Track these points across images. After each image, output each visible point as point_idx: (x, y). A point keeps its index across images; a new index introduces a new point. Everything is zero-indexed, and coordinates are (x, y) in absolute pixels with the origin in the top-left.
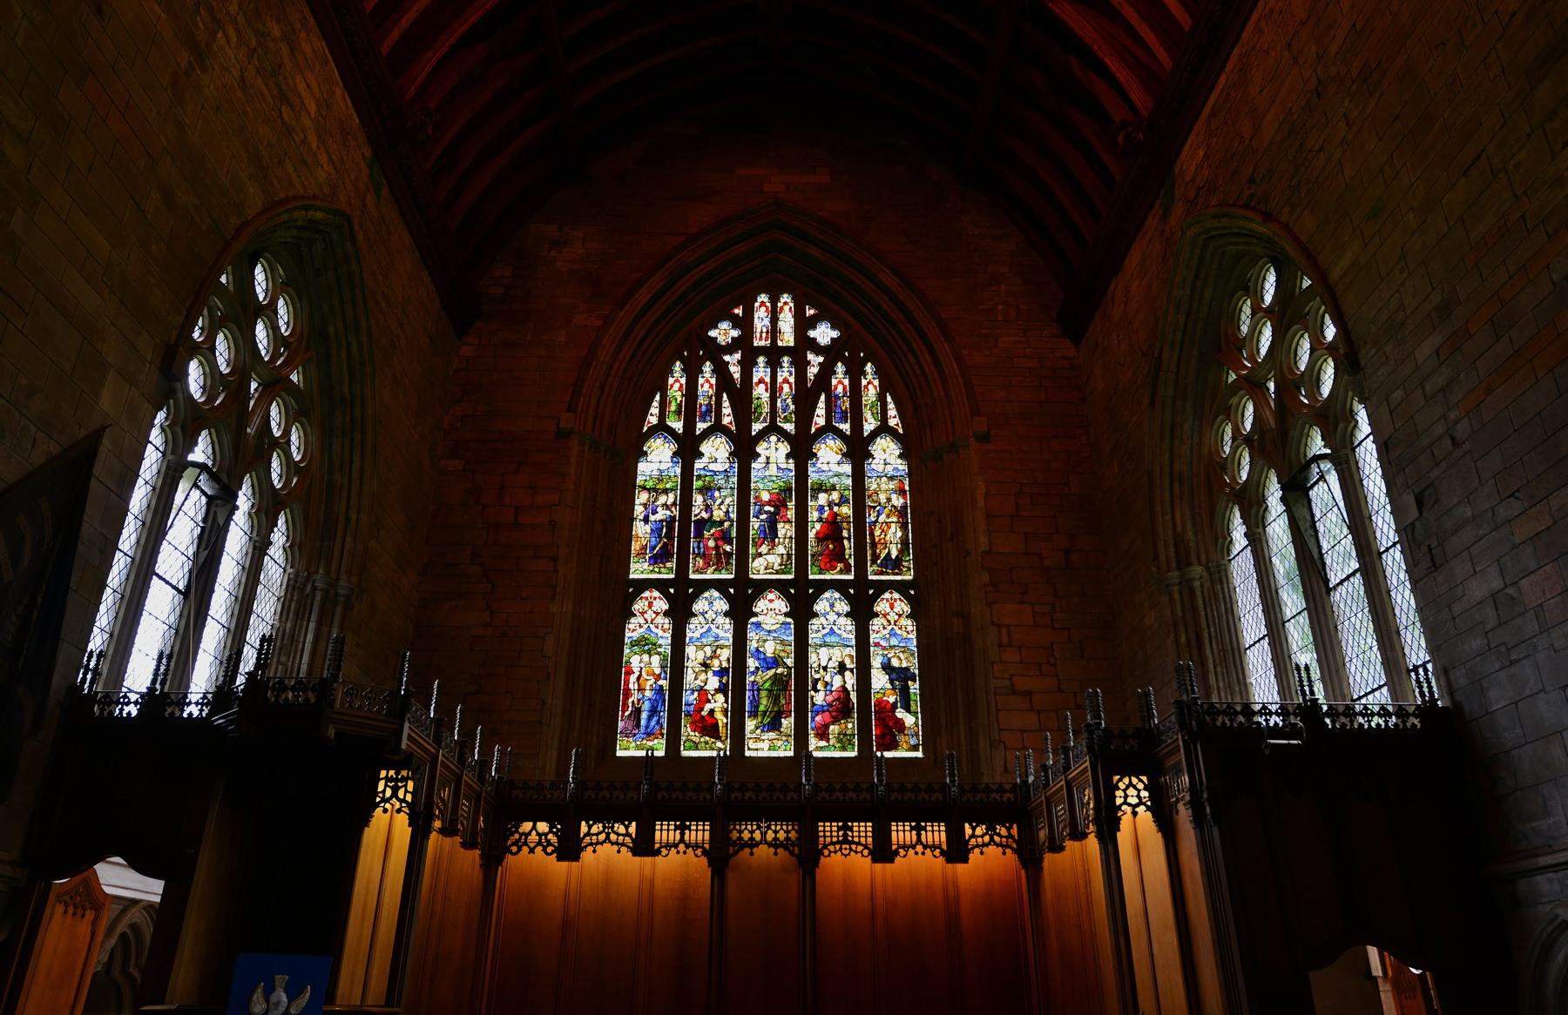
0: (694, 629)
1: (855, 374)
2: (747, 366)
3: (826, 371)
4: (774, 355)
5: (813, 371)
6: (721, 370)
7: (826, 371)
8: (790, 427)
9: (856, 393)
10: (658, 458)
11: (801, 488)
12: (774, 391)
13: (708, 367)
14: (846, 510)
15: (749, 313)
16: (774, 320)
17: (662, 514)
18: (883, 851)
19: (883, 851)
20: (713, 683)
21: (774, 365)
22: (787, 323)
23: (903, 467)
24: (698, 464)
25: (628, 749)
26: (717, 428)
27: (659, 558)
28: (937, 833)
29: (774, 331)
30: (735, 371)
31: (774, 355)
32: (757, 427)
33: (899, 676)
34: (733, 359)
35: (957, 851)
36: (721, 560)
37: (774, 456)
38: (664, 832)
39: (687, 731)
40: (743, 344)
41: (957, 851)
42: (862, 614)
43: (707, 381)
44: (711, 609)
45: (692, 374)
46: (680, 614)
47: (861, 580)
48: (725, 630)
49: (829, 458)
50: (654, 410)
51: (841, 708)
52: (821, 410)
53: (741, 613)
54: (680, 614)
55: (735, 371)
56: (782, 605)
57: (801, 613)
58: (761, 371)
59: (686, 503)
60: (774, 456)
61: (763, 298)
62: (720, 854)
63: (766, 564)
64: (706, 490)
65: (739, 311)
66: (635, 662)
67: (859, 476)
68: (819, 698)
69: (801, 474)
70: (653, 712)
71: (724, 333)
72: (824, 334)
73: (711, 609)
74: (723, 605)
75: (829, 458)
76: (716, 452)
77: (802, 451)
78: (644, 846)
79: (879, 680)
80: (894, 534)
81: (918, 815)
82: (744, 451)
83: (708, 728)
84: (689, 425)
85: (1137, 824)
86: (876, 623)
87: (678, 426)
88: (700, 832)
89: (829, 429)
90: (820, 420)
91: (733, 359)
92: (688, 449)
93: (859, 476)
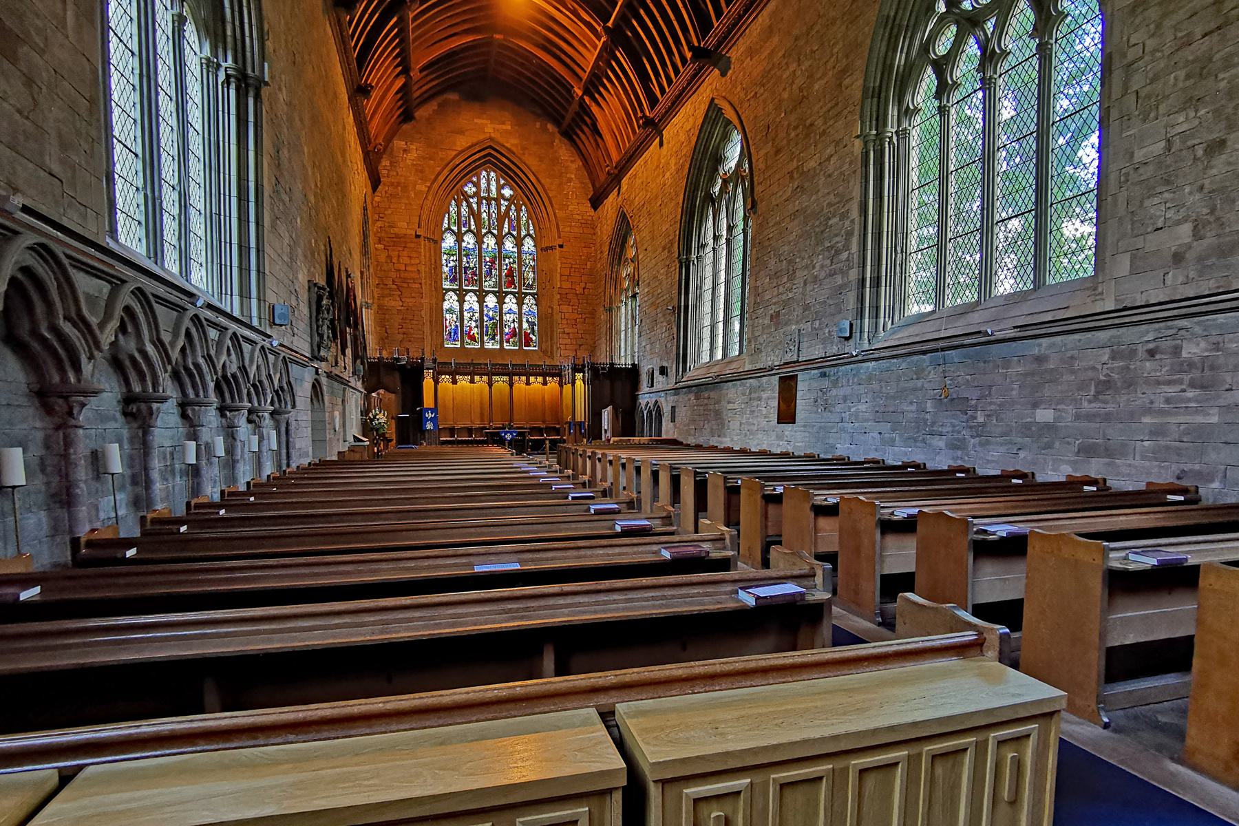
0: (466, 306)
1: (518, 210)
2: (479, 204)
3: (508, 208)
4: (489, 199)
5: (503, 208)
6: (469, 205)
7: (508, 208)
8: (495, 232)
9: (519, 218)
10: (449, 241)
11: (500, 255)
12: (489, 216)
13: (464, 204)
14: (515, 266)
15: (479, 180)
16: (489, 185)
17: (452, 264)
18: (528, 383)
19: (528, 383)
20: (473, 324)
21: (489, 204)
22: (493, 188)
23: (533, 249)
24: (464, 245)
25: (448, 345)
26: (470, 230)
27: (453, 280)
28: (540, 379)
29: (489, 190)
30: (475, 206)
31: (489, 199)
32: (484, 231)
33: (531, 324)
34: (473, 201)
35: (545, 383)
36: (473, 283)
37: (490, 242)
38: (477, 378)
39: (466, 339)
40: (477, 194)
41: (545, 383)
42: (520, 304)
43: (464, 210)
44: (471, 300)
45: (459, 206)
46: (461, 301)
47: (520, 292)
48: (476, 307)
49: (509, 245)
50: (446, 221)
51: (513, 334)
52: (506, 225)
53: (481, 301)
54: (461, 301)
55: (475, 206)
56: (495, 299)
57: (501, 302)
58: (484, 207)
59: (460, 261)
60: (490, 242)
61: (484, 173)
62: (490, 385)
63: (488, 285)
64: (467, 256)
65: (475, 179)
66: (448, 316)
67: (519, 252)
68: (507, 330)
69: (500, 252)
70: (455, 333)
71: (470, 189)
72: (507, 192)
73: (471, 300)
74: (475, 298)
75: (509, 245)
76: (469, 240)
77: (500, 243)
78: (472, 381)
79: (525, 325)
80: (531, 275)
81: (536, 375)
82: (479, 241)
83: (472, 338)
84: (459, 229)
85: (579, 383)
86: (525, 307)
87: (455, 228)
88: (485, 378)
89: (509, 233)
90: (506, 230)
91: (473, 201)
92: (459, 239)
93: (519, 252)
